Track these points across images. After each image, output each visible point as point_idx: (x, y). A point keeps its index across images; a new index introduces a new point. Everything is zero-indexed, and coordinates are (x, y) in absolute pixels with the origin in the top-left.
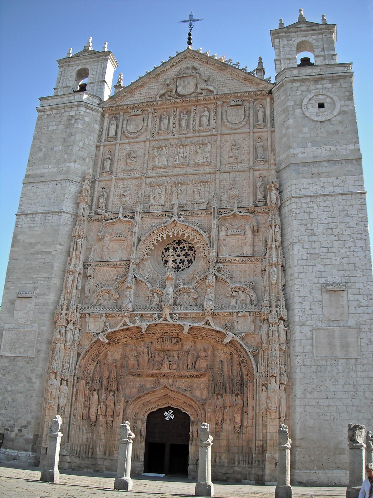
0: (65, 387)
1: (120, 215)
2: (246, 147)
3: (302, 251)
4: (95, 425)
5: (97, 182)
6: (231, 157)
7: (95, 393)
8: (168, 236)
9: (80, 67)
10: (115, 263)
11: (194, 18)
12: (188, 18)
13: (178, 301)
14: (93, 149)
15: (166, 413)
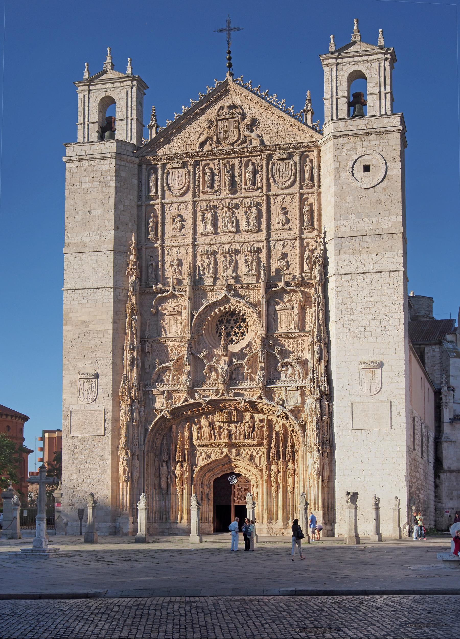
0: (137, 462)
1: (171, 289)
2: (293, 211)
3: (341, 330)
4: (167, 493)
5: (144, 249)
6: (279, 223)
7: (164, 464)
8: (220, 310)
9: (103, 95)
10: (172, 339)
11: (233, 25)
12: (225, 26)
13: (234, 376)
14: (135, 210)
15: (229, 478)
